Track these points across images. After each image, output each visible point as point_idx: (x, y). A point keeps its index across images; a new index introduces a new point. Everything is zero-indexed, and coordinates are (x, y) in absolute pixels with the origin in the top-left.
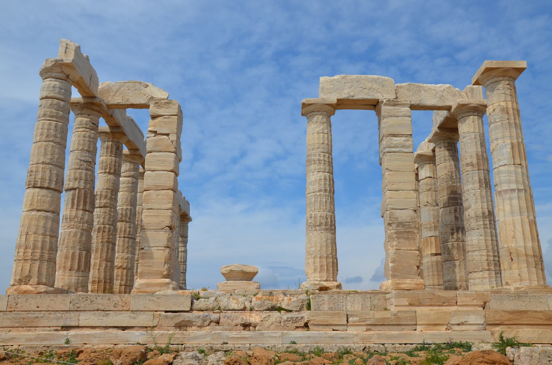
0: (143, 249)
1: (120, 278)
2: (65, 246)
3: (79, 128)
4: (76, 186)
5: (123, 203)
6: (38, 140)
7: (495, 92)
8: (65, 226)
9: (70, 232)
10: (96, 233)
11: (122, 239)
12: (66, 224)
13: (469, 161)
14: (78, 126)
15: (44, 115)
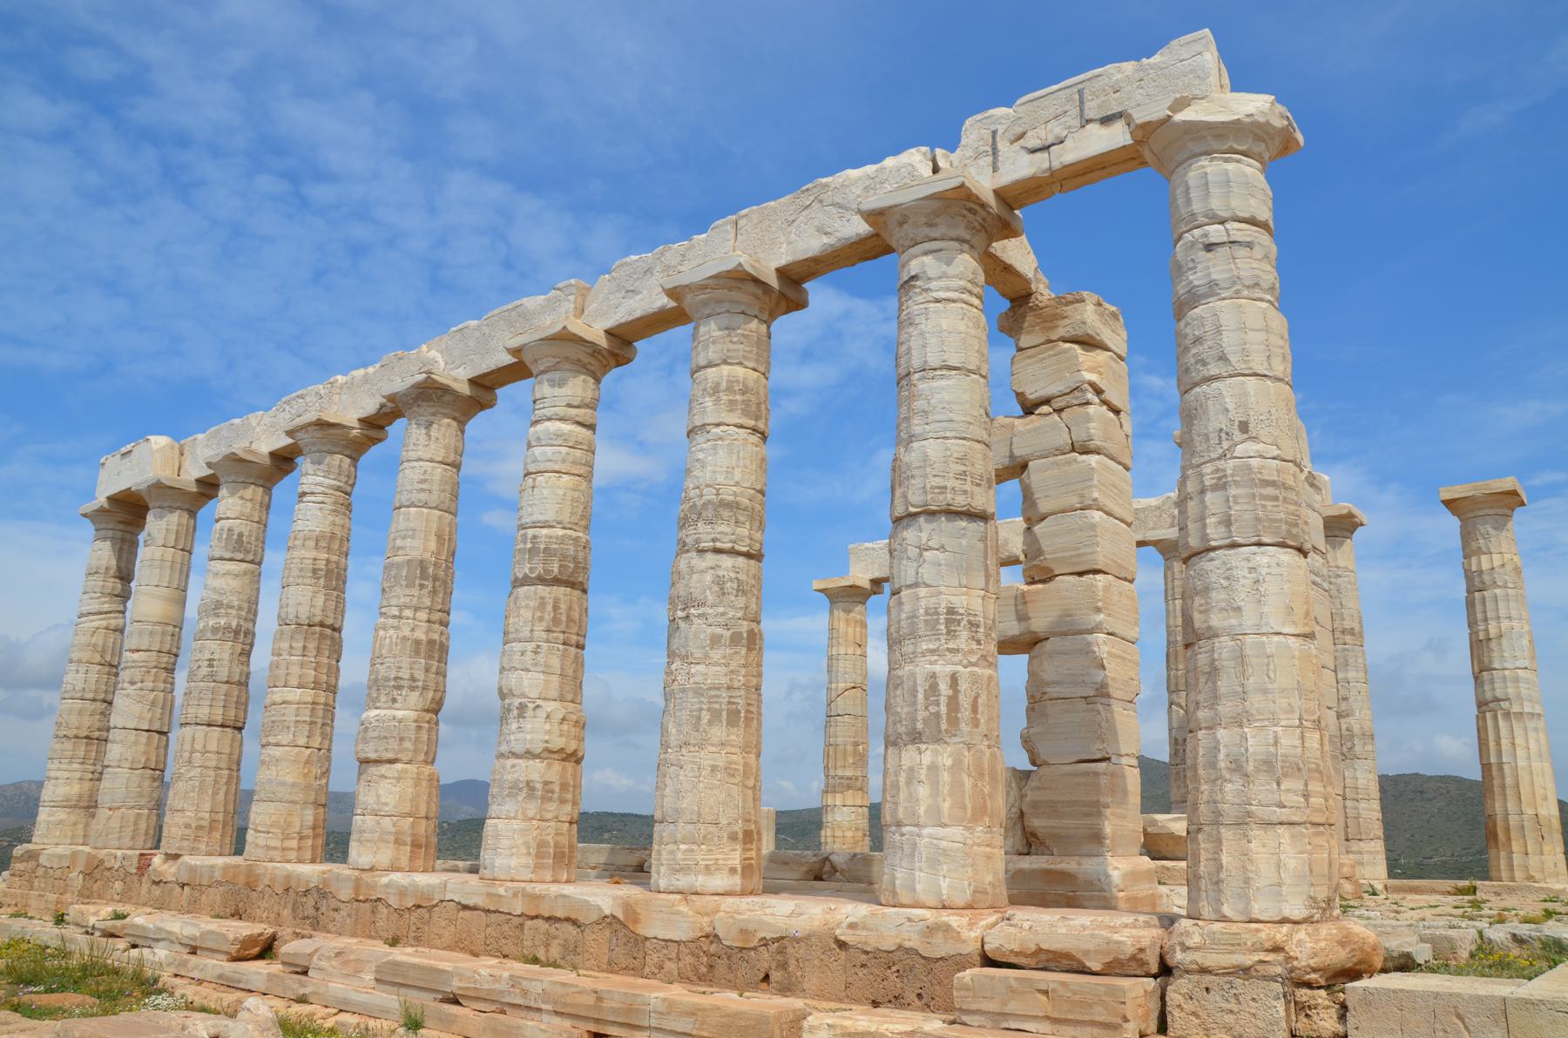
0: (1108, 759)
1: (569, 796)
2: (983, 728)
3: (970, 292)
4: (991, 510)
5: (575, 519)
6: (1280, 375)
7: (1504, 533)
8: (971, 652)
9: (990, 678)
10: (744, 651)
11: (573, 650)
12: (975, 647)
13: (1347, 624)
14: (969, 286)
15: (1273, 288)
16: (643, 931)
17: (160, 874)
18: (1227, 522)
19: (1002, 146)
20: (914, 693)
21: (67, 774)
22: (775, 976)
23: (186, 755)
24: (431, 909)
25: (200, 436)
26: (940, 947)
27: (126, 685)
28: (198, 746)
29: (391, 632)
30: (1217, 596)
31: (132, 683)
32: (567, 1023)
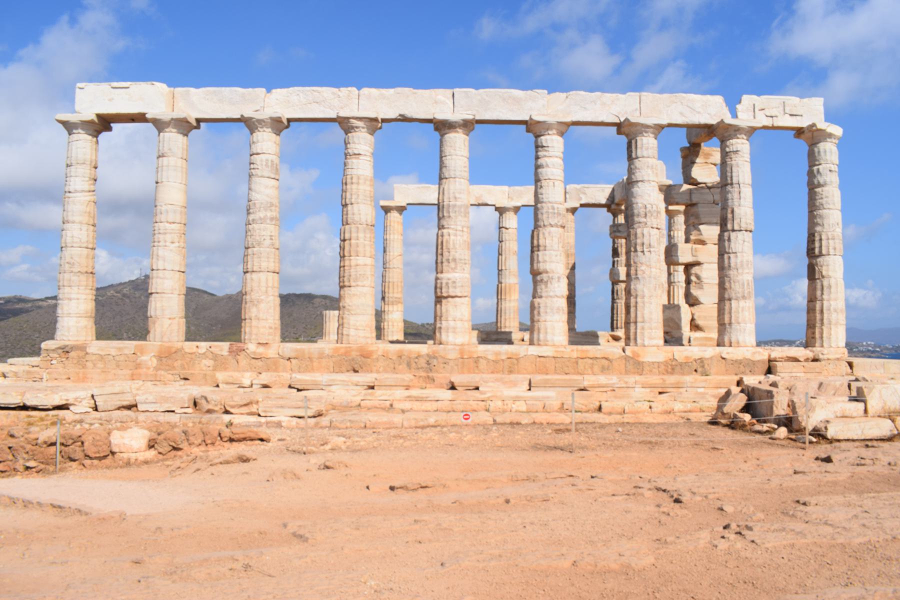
16: (641, 359)
17: (261, 354)
18: (835, 249)
19: (756, 110)
20: (743, 285)
21: (84, 297)
22: (699, 370)
23: (264, 289)
24: (517, 359)
25: (192, 90)
26: (757, 358)
27: (168, 244)
28: (270, 284)
29: (459, 238)
30: (831, 267)
31: (173, 243)
32: (648, 390)
